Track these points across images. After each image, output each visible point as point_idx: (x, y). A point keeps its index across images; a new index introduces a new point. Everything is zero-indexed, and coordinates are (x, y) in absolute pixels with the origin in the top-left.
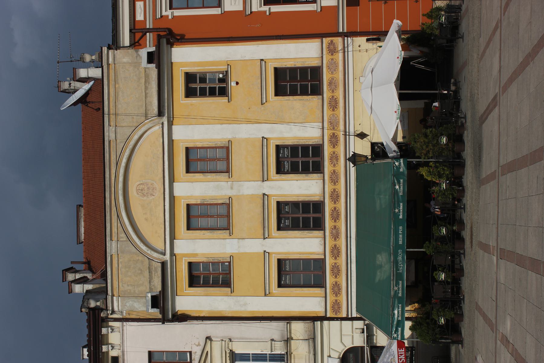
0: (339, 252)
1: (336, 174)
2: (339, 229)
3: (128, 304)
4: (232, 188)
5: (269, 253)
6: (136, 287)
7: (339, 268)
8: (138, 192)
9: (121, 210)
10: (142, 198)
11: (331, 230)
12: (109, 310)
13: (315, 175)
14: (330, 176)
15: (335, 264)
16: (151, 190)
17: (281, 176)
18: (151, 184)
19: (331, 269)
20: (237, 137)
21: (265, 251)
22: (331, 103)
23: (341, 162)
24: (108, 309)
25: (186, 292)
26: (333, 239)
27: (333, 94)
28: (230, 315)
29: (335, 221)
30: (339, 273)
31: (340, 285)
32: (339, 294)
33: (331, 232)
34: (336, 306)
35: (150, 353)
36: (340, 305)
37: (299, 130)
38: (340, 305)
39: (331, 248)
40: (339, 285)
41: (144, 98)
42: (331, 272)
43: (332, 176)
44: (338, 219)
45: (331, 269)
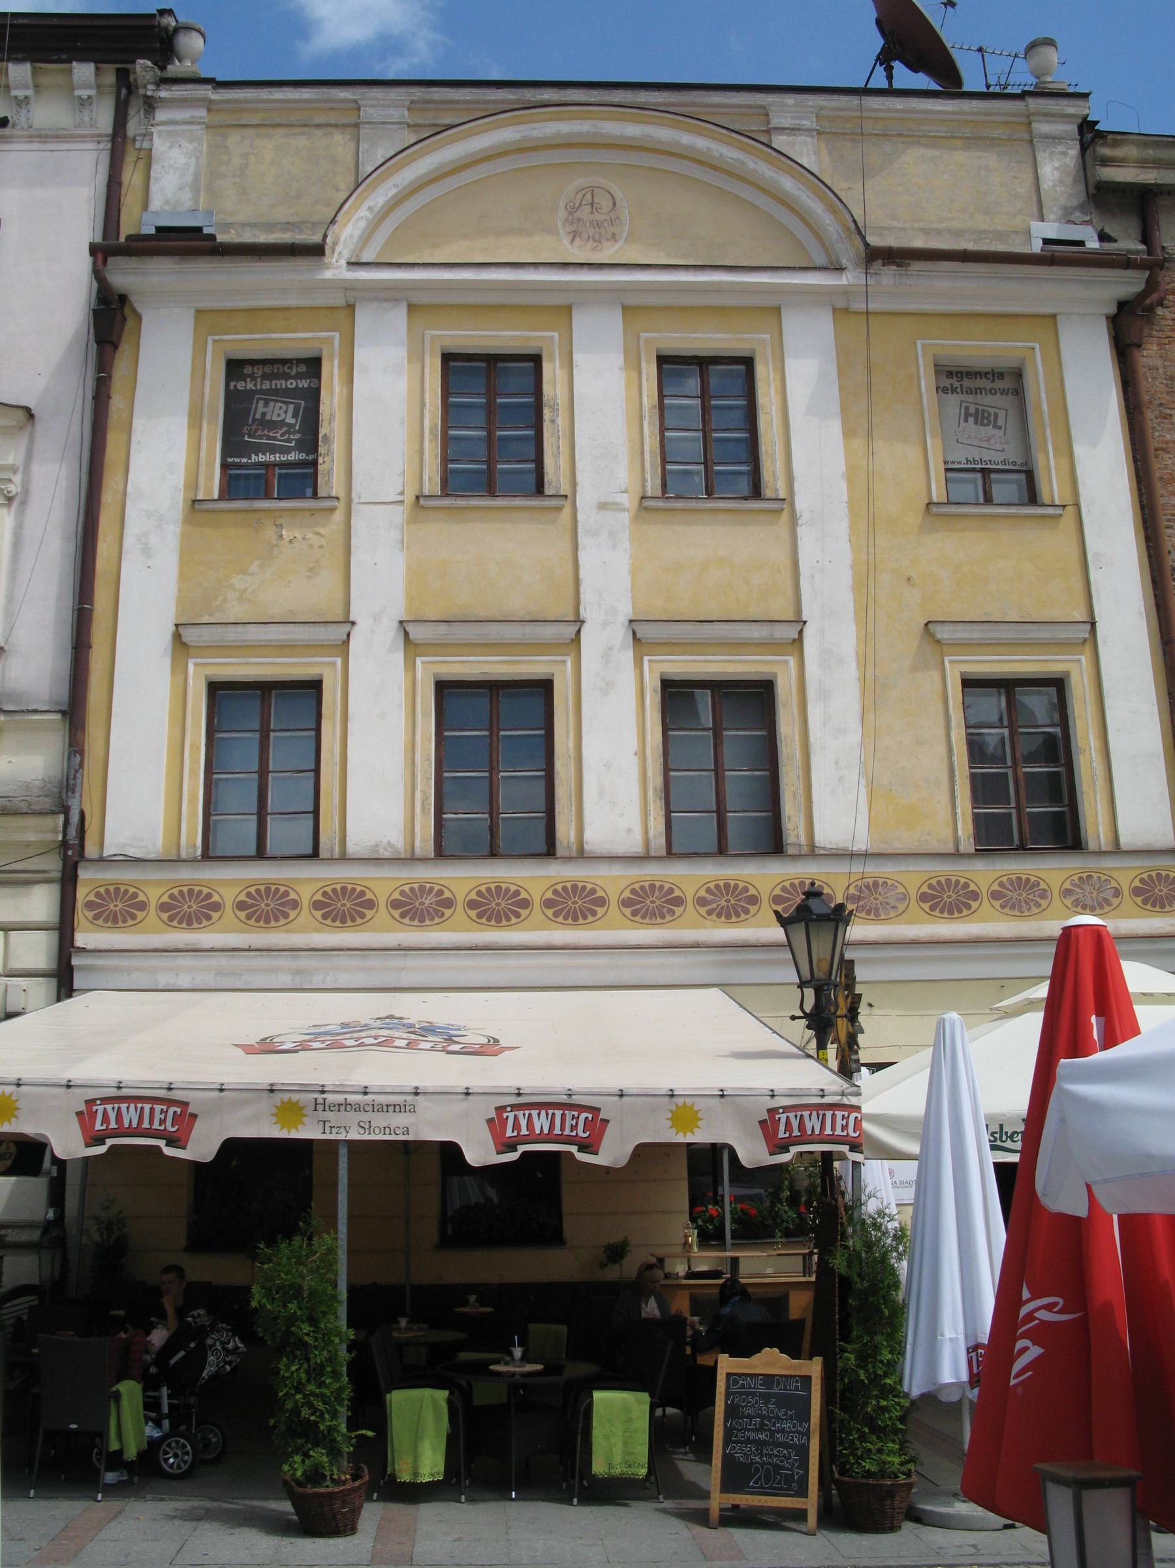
0: (343, 921)
1: (665, 911)
2: (437, 920)
4: (603, 506)
5: (346, 642)
6: (237, 180)
7: (277, 920)
8: (584, 191)
9: (522, 127)
10: (562, 205)
11: (437, 888)
12: (158, 90)
14: (658, 884)
15: (295, 904)
16: (591, 232)
17: (655, 691)
18: (614, 235)
19: (273, 888)
21: (353, 623)
22: (949, 888)
23: (714, 927)
24: (163, 87)
25: (210, 343)
26: (396, 896)
27: (985, 895)
28: (108, 497)
29: (472, 905)
30: (258, 921)
31: (205, 923)
32: (171, 919)
33: (428, 886)
36: (125, 921)
37: (837, 763)
38: (125, 921)
39: (359, 889)
40: (209, 918)
41: (922, 225)
42: (262, 888)
43: (657, 894)
44: (480, 916)
45: (273, 888)
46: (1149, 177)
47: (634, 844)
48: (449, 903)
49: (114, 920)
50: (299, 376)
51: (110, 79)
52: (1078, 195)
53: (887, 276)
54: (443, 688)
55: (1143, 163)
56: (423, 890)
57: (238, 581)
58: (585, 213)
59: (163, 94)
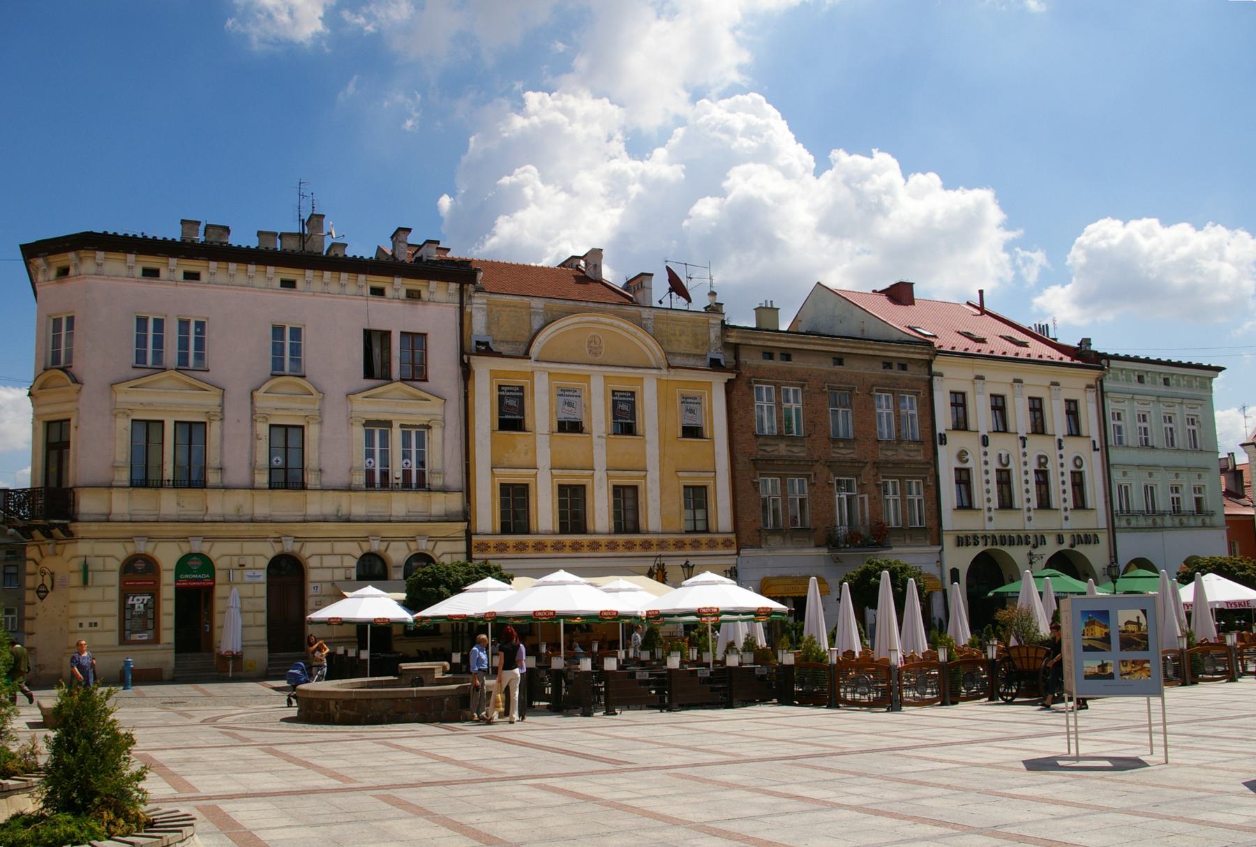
3: (479, 314)
4: (599, 437)
13: (612, 525)
15: (528, 546)
20: (647, 445)
28: (470, 428)
34: (484, 547)
35: (425, 335)
46: (738, 341)
47: (607, 530)
48: (565, 546)
49: (482, 551)
50: (517, 391)
51: (458, 286)
52: (719, 345)
53: (673, 371)
54: (560, 486)
55: (737, 337)
56: (559, 542)
57: (506, 455)
58: (592, 344)
59: (476, 295)
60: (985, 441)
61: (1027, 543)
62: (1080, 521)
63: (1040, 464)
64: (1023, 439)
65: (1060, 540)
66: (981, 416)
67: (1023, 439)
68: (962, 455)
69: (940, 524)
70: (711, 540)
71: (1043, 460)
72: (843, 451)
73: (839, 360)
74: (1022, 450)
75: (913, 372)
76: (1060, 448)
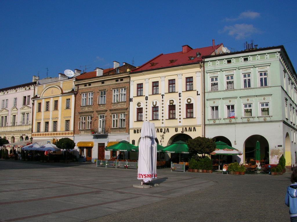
60: (147, 98)
61: (161, 131)
62: (190, 122)
63: (170, 103)
64: (163, 95)
65: (176, 130)
66: (147, 89)
67: (163, 95)
68: (139, 104)
69: (129, 127)
70: (69, 133)
71: (172, 102)
72: (102, 107)
73: (103, 82)
74: (162, 99)
75: (125, 80)
76: (179, 96)
